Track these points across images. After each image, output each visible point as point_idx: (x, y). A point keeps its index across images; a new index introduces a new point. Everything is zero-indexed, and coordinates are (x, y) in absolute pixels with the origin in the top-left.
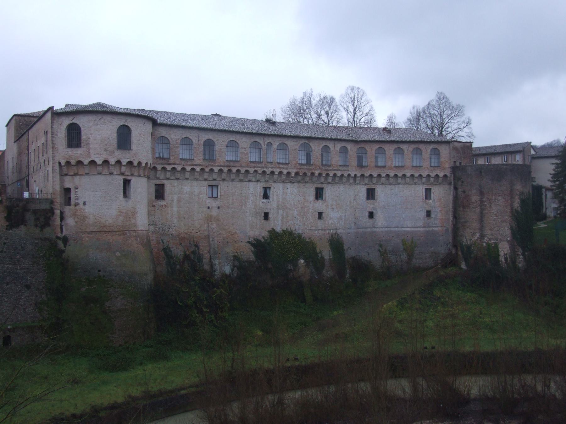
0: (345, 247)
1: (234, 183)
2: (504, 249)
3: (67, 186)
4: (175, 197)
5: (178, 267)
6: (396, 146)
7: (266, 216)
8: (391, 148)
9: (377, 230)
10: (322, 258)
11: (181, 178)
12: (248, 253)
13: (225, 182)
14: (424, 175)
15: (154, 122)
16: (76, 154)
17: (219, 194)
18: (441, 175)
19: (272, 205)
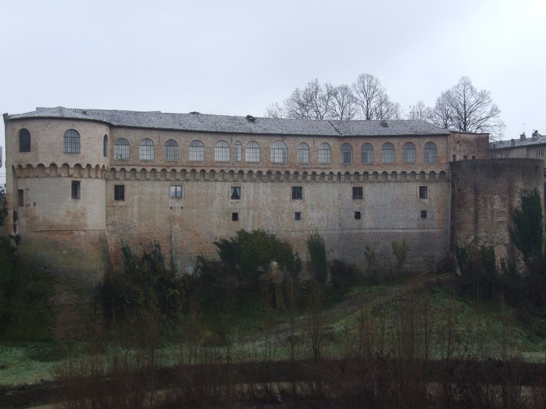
0: (327, 249)
1: (199, 182)
2: (501, 253)
3: (21, 187)
4: (136, 198)
5: (137, 267)
6: (385, 141)
7: (235, 217)
8: (379, 143)
9: (365, 231)
10: (299, 260)
11: (142, 179)
12: (213, 254)
13: (189, 182)
14: (418, 172)
15: (111, 126)
16: (27, 158)
17: (183, 194)
18: (438, 171)
19: (240, 206)
